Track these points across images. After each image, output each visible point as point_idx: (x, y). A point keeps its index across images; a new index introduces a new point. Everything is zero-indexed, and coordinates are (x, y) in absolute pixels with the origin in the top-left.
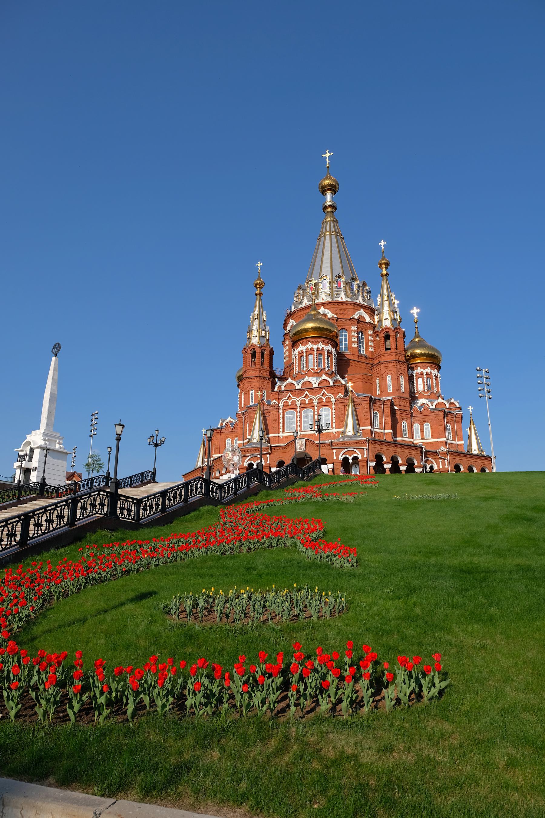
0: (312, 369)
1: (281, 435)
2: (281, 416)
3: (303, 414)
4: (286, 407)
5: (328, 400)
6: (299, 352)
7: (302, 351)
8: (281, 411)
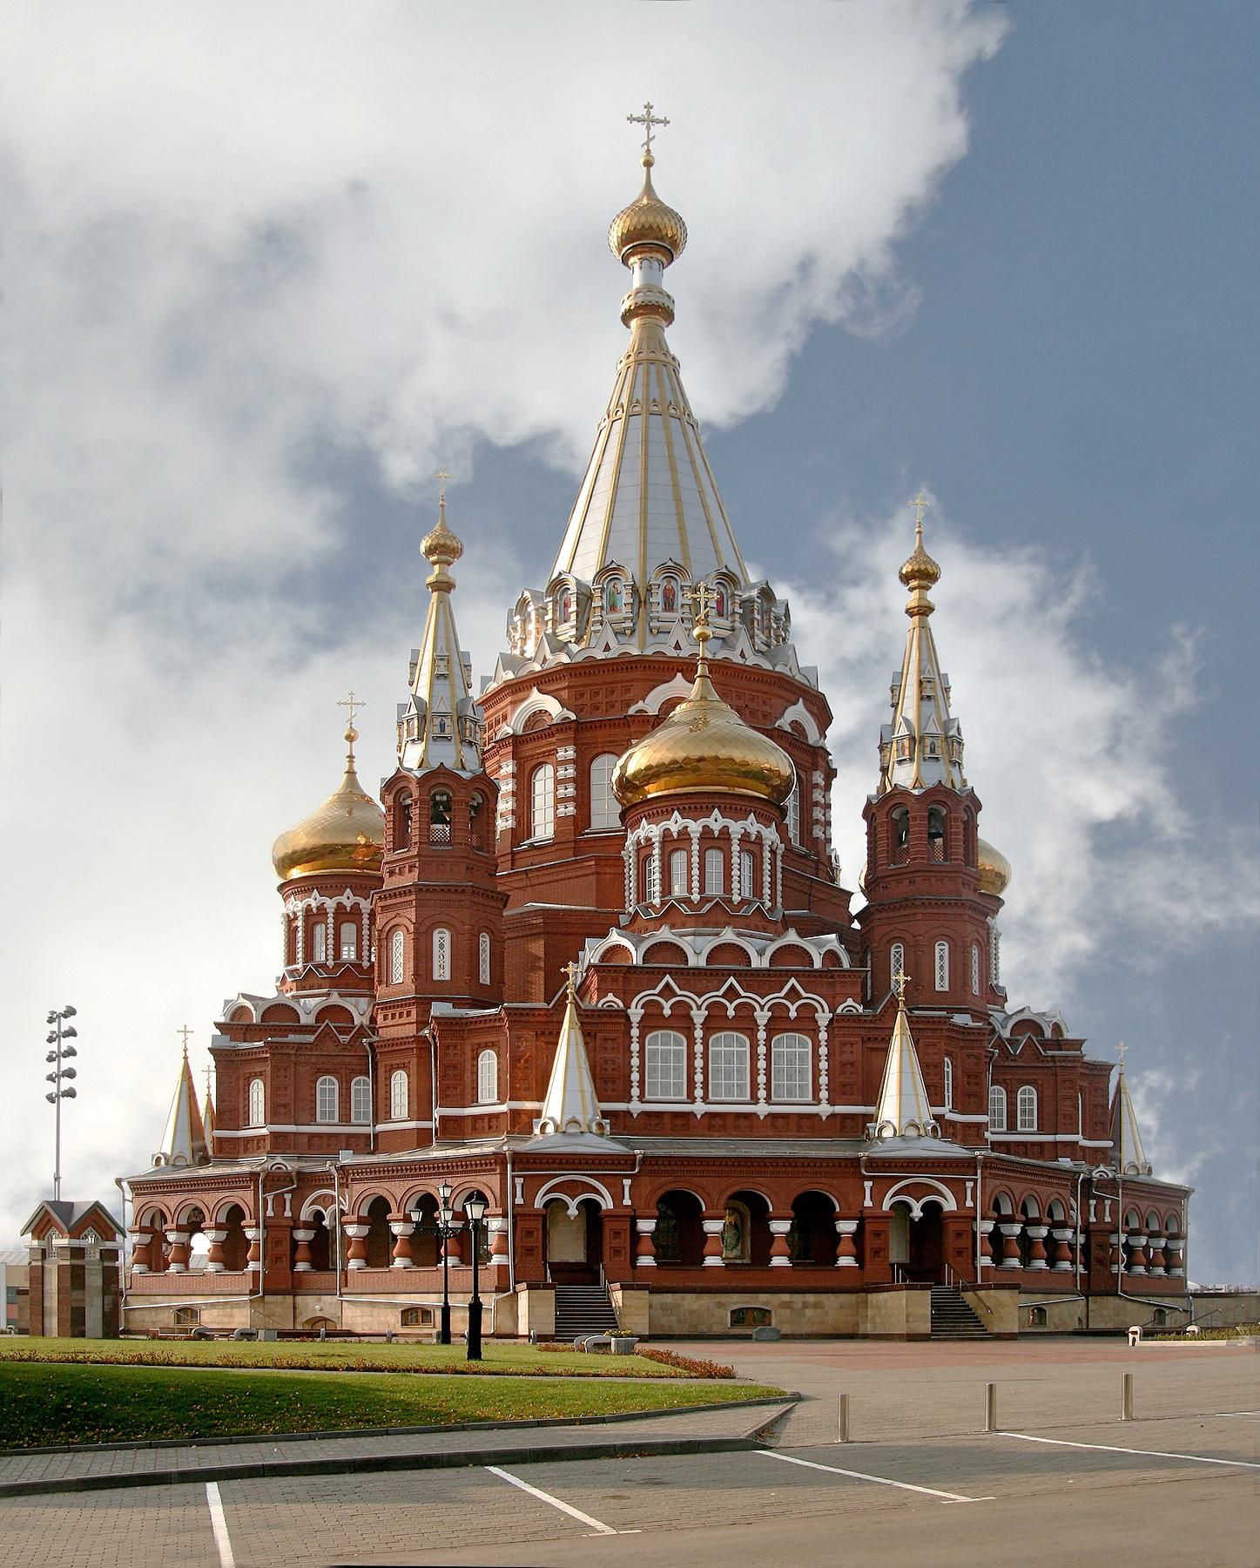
0: (680, 901)
1: (636, 1107)
2: (635, 1047)
3: (647, 1047)
4: (653, 1020)
5: (808, 1013)
6: (638, 843)
8: (635, 1032)
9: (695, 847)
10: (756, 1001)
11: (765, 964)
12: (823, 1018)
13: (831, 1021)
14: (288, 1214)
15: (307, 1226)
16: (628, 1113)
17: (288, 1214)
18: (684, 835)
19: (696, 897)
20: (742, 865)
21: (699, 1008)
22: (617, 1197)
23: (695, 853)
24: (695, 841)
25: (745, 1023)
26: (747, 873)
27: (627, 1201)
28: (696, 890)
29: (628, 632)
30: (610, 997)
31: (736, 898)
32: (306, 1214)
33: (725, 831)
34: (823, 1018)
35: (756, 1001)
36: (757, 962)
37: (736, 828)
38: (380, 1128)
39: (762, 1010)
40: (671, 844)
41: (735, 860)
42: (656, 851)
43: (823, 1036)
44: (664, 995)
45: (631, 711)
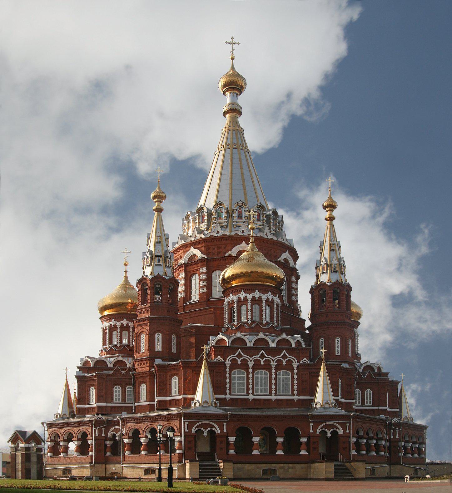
0: (244, 323)
1: (228, 397)
2: (228, 375)
3: (232, 375)
4: (234, 366)
5: (290, 363)
6: (229, 302)
7: (232, 301)
8: (228, 370)
9: (249, 304)
10: (271, 359)
11: (275, 345)
12: (295, 365)
13: (298, 366)
14: (103, 435)
15: (110, 439)
16: (225, 399)
17: (103, 435)
18: (245, 299)
19: (250, 321)
20: (266, 310)
21: (251, 361)
22: (221, 429)
23: (249, 306)
24: (249, 301)
25: (267, 366)
26: (268, 313)
27: (225, 431)
28: (250, 319)
29: (225, 226)
30: (219, 357)
31: (264, 322)
32: (109, 435)
33: (260, 298)
34: (295, 365)
35: (271, 359)
36: (271, 345)
37: (264, 297)
38: (136, 404)
39: (273, 362)
40: (241, 302)
41: (264, 308)
42: (235, 305)
43: (295, 371)
44: (239, 356)
45: (227, 255)
